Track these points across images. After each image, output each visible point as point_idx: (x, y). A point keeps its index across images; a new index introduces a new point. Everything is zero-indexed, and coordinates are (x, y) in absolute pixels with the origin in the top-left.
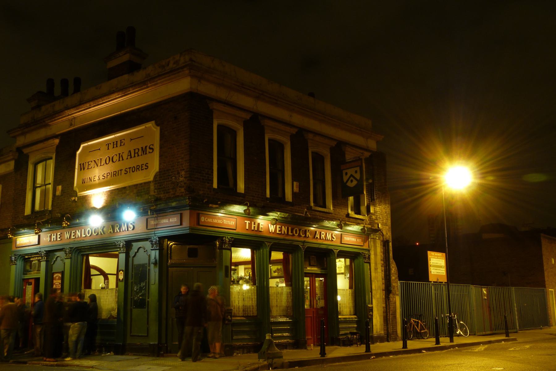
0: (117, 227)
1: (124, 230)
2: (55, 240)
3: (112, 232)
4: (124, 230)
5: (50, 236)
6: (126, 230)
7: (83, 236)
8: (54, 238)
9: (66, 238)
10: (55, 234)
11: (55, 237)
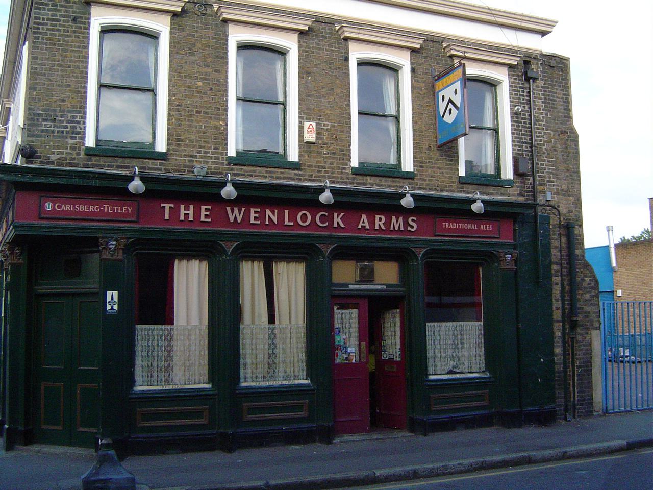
0: (380, 219)
1: (397, 229)
2: (191, 218)
3: (367, 227)
4: (397, 229)
5: (170, 207)
6: (402, 229)
7: (286, 223)
8: (187, 215)
9: (232, 221)
10: (191, 207)
11: (191, 212)
